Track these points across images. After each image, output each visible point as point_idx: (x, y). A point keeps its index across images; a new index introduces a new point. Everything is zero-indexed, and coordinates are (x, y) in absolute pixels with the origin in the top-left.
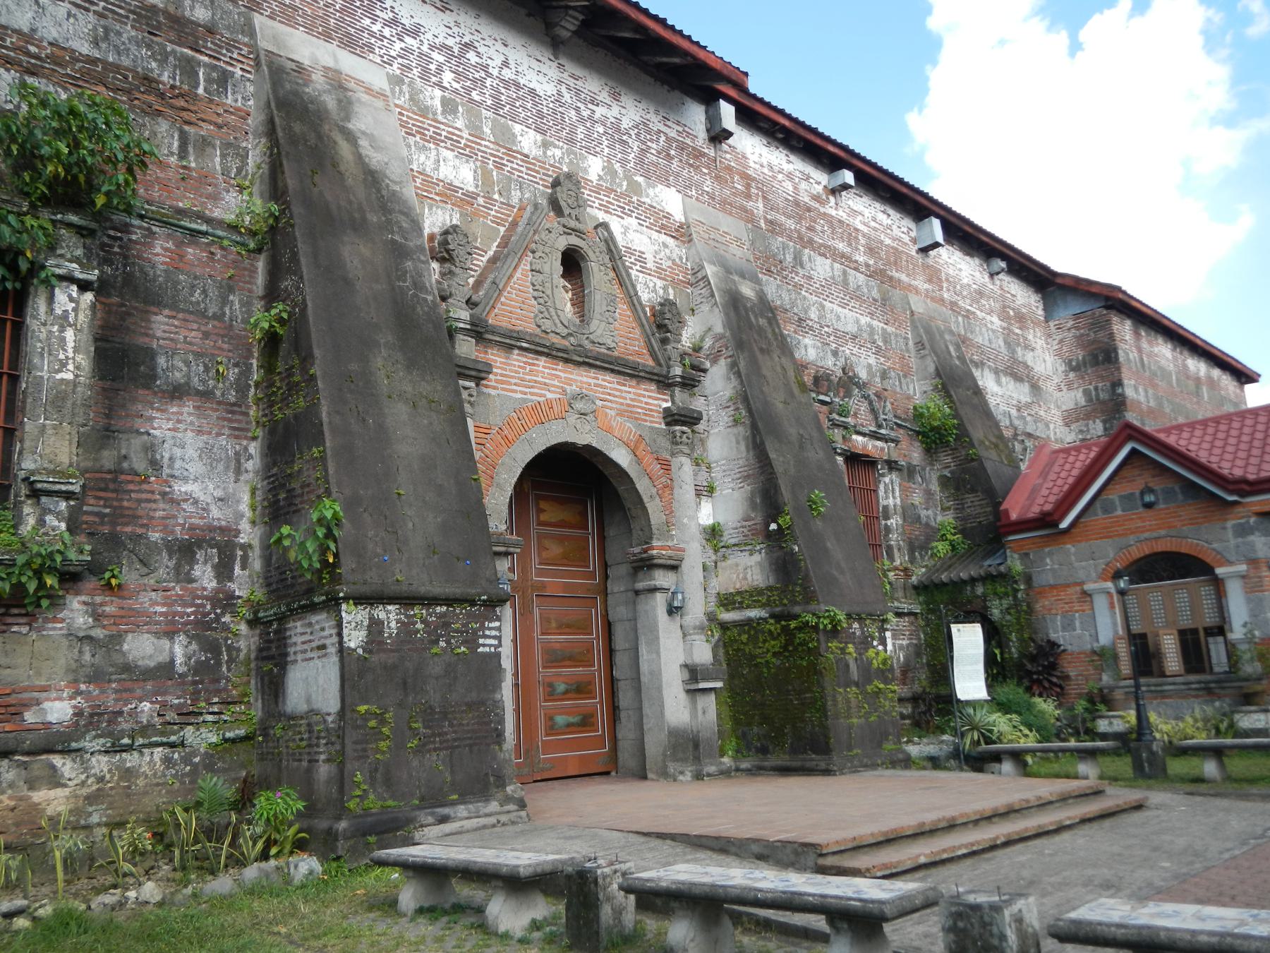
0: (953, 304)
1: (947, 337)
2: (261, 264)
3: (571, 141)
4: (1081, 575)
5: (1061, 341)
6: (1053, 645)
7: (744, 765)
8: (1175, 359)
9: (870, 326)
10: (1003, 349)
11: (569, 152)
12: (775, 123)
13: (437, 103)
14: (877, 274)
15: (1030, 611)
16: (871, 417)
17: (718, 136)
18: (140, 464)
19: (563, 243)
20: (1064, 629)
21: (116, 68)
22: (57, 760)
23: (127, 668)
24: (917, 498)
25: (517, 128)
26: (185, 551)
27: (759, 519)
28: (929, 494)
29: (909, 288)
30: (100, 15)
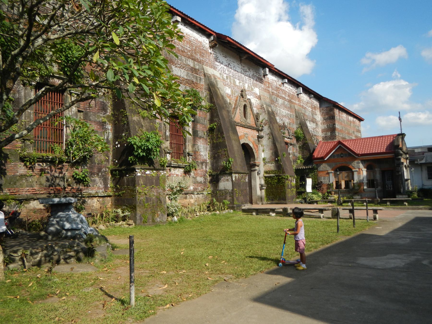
0: (303, 106)
1: (302, 114)
2: (208, 114)
3: (243, 81)
4: (328, 169)
5: (323, 113)
6: (321, 182)
7: (269, 203)
8: (346, 117)
9: (288, 113)
10: (311, 116)
11: (243, 83)
12: (274, 71)
13: (225, 78)
14: (290, 101)
15: (317, 176)
16: (288, 134)
17: (265, 75)
18: (197, 150)
19: (244, 103)
20: (323, 179)
21: (189, 80)
22: (192, 195)
23: (197, 182)
24: (295, 151)
25: (236, 80)
26: (202, 163)
27: (274, 157)
28: (297, 150)
29: (295, 103)
30: (187, 71)
